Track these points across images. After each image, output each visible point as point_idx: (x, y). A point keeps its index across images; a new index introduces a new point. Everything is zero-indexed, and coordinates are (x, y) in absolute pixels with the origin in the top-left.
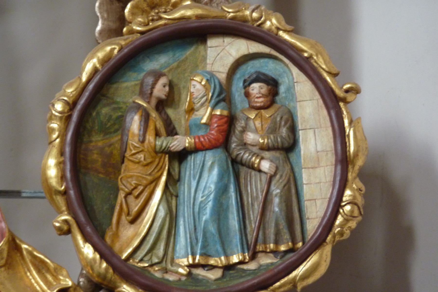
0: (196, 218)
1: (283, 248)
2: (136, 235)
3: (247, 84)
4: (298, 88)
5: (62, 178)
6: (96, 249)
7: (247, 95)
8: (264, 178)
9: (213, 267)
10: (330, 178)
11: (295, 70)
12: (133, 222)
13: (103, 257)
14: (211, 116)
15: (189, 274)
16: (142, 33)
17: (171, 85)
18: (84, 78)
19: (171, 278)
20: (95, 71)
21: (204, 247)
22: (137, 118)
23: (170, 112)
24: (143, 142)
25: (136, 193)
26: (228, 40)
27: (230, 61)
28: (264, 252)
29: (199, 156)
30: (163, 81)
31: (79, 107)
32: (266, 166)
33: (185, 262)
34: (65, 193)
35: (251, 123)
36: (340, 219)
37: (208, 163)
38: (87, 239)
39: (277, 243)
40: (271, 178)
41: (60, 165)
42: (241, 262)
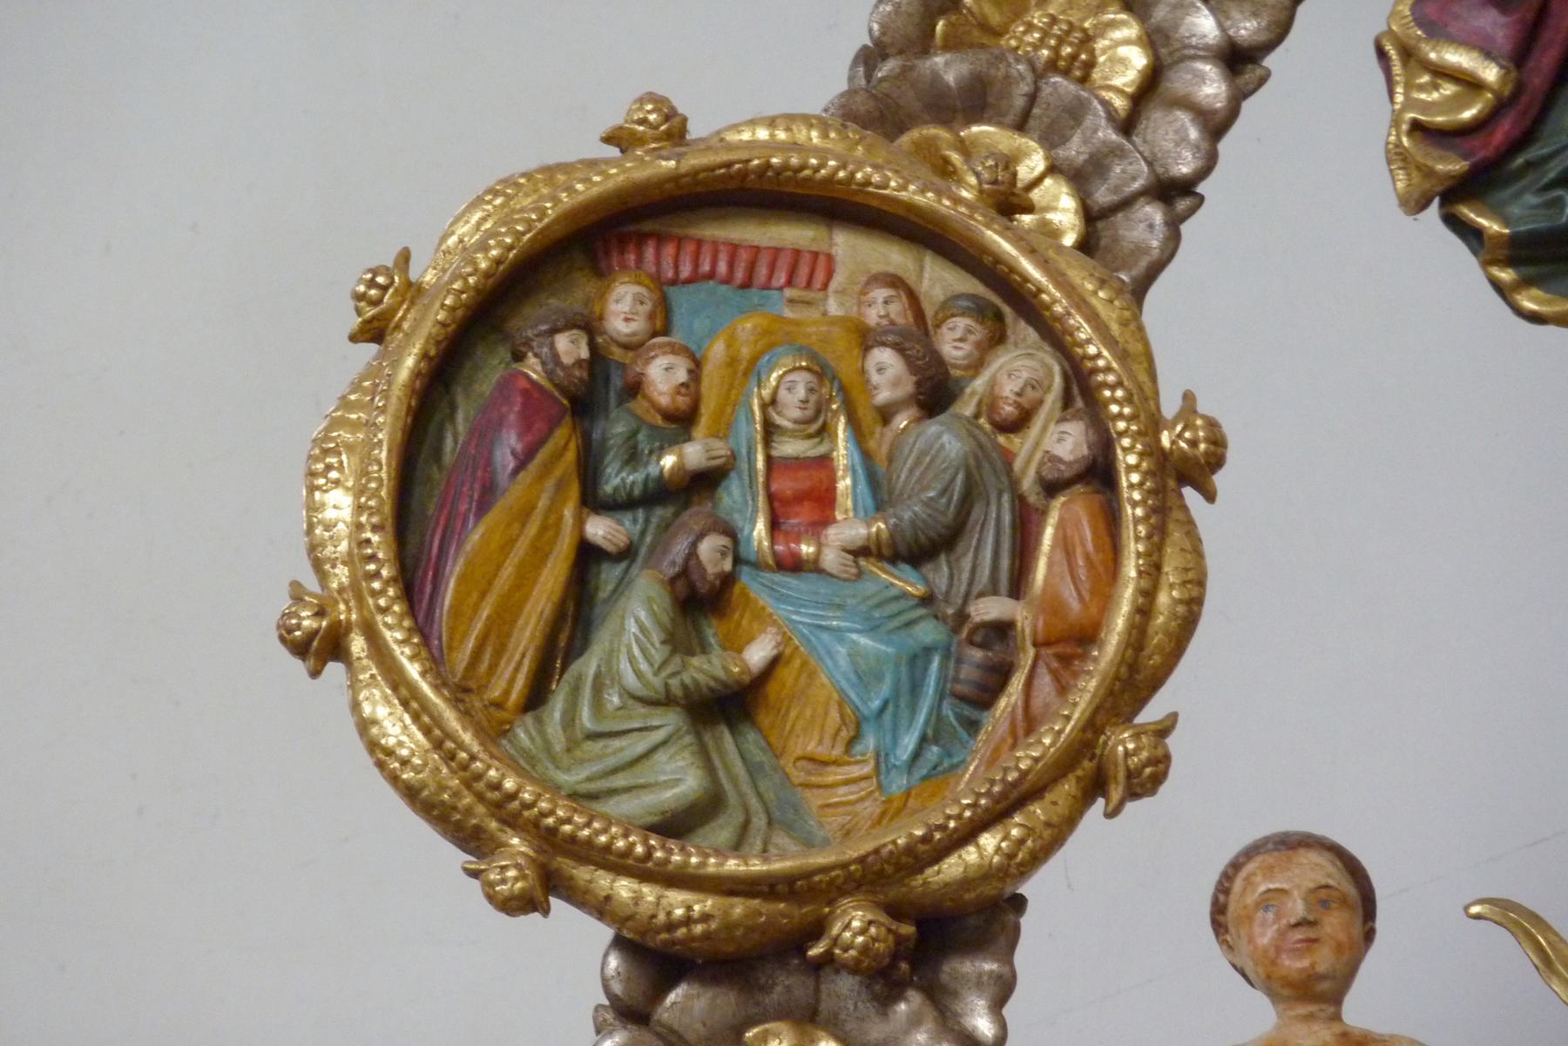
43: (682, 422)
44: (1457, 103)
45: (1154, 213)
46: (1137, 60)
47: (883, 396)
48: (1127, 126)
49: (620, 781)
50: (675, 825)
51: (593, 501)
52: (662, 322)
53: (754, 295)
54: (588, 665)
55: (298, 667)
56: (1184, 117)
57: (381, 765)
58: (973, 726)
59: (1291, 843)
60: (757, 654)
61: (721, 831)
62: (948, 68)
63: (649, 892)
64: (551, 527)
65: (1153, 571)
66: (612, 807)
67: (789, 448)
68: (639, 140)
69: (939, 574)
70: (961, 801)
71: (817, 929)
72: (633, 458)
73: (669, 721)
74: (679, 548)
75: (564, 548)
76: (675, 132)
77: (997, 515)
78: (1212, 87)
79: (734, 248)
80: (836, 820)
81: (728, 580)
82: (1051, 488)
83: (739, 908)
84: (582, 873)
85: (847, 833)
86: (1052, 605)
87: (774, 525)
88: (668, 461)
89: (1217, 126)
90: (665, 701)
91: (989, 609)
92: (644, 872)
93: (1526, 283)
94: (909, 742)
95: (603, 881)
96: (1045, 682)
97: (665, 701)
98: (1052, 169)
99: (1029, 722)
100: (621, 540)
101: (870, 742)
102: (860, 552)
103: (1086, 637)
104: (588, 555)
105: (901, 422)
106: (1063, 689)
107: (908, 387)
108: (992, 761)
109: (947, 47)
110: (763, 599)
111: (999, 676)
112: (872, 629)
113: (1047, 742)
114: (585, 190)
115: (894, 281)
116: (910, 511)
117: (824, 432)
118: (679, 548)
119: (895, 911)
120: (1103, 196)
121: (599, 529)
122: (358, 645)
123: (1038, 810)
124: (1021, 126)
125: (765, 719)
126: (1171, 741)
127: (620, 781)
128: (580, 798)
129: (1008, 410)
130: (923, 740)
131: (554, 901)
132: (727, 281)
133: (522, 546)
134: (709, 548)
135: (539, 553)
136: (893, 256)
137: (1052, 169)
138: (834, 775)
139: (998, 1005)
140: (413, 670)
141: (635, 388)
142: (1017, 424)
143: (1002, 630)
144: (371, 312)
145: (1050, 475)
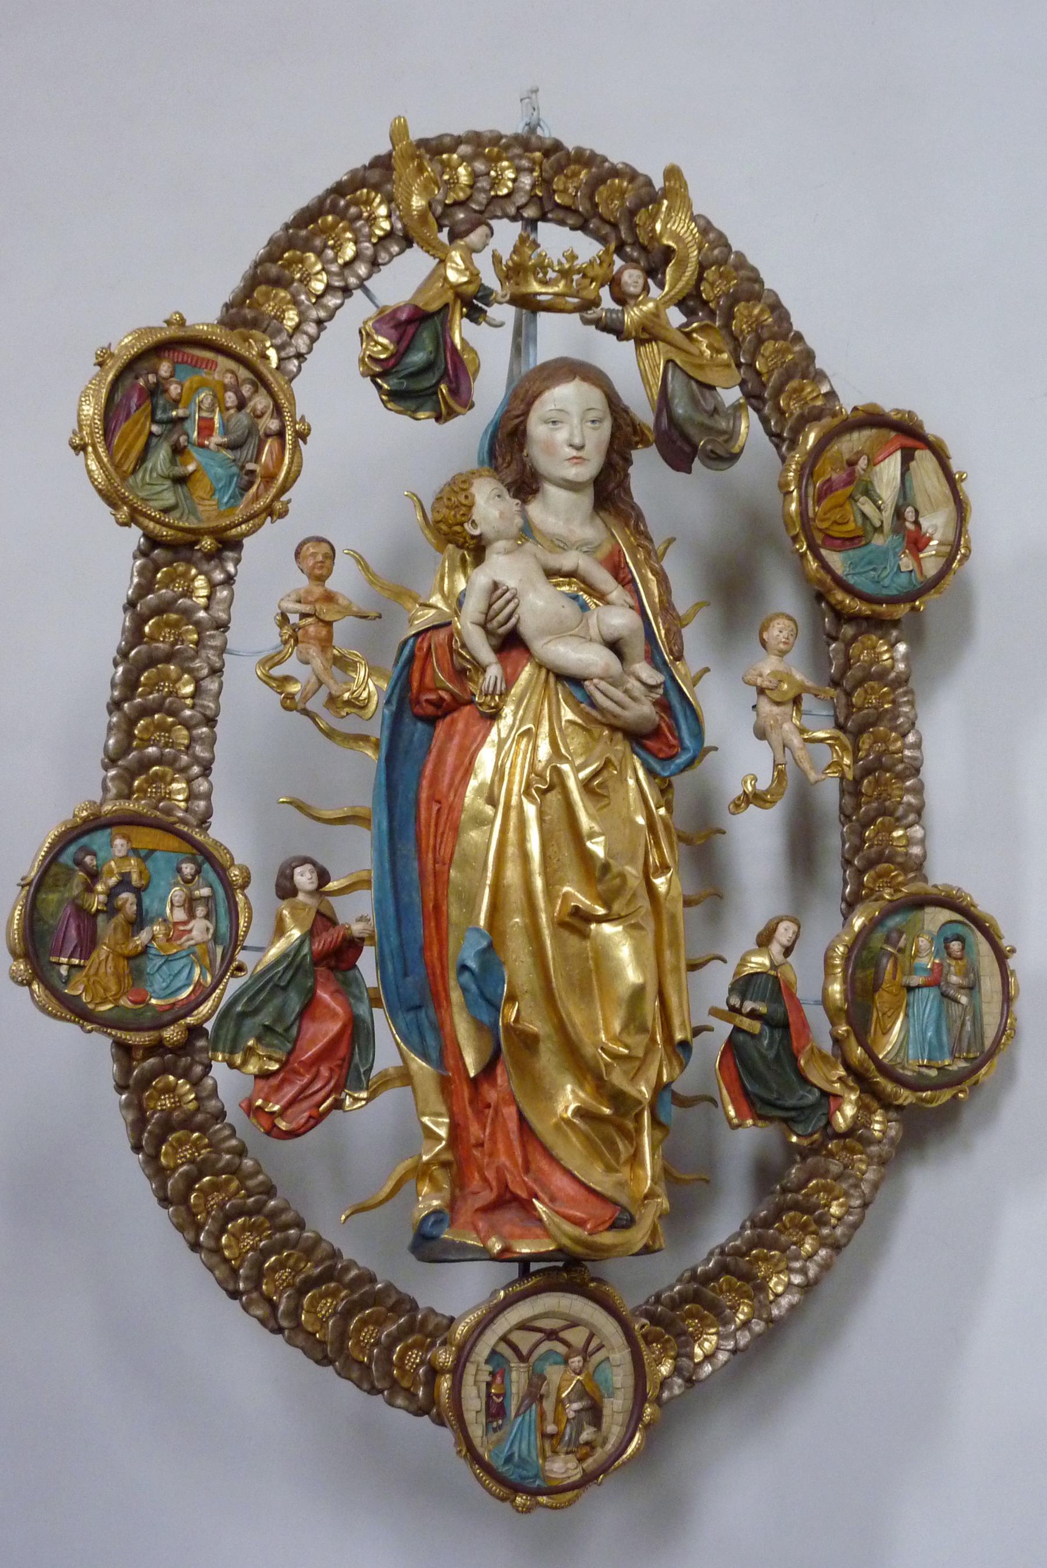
1: (972, 1056)
5: (846, 999)
11: (979, 934)
14: (934, 964)
16: (890, 901)
19: (909, 1073)
21: (929, 1053)
24: (894, 978)
25: (889, 1014)
26: (938, 909)
31: (855, 952)
32: (964, 1000)
35: (952, 968)
36: (1004, 1037)
37: (932, 996)
39: (968, 1052)
44: (380, 352)
45: (296, 362)
47: (229, 404)
48: (291, 337)
49: (154, 497)
50: (166, 511)
51: (154, 421)
53: (197, 369)
54: (149, 465)
55: (72, 451)
56: (305, 336)
57: (93, 483)
58: (242, 495)
59: (320, 540)
60: (191, 468)
61: (177, 514)
62: (249, 313)
63: (158, 527)
64: (144, 424)
65: (291, 462)
66: (151, 503)
67: (205, 414)
68: (173, 324)
69: (238, 453)
70: (238, 515)
71: (197, 542)
72: (164, 411)
73: (168, 483)
74: (175, 437)
75: (146, 432)
76: (182, 323)
77: (253, 442)
79: (193, 356)
80: (206, 514)
81: (185, 447)
82: (268, 436)
83: (180, 534)
84: (141, 519)
85: (208, 518)
88: (174, 413)
89: (313, 339)
90: (167, 478)
91: (250, 466)
92: (158, 521)
93: (389, 401)
94: (225, 499)
95: (146, 522)
96: (262, 487)
97: (167, 478)
98: (272, 346)
99: (257, 497)
100: (160, 432)
101: (217, 497)
102: (219, 445)
104: (151, 434)
105: (232, 411)
107: (236, 403)
108: (246, 506)
109: (249, 307)
110: (195, 455)
111: (250, 484)
112: (221, 467)
113: (262, 503)
114: (160, 336)
115: (233, 372)
116: (233, 437)
117: (213, 411)
118: (175, 437)
120: (283, 354)
121: (155, 429)
122: (90, 449)
123: (256, 520)
124: (264, 332)
125: (189, 484)
126: (289, 505)
127: (154, 497)
128: (144, 500)
129: (259, 413)
130: (230, 498)
131: (133, 525)
132: (191, 364)
133: (136, 431)
134: (182, 439)
135: (140, 433)
136: (232, 364)
137: (272, 346)
138: (207, 502)
139: (236, 564)
140: (105, 460)
141: (166, 391)
142: (260, 417)
143: (252, 472)
144: (101, 359)
145: (268, 431)
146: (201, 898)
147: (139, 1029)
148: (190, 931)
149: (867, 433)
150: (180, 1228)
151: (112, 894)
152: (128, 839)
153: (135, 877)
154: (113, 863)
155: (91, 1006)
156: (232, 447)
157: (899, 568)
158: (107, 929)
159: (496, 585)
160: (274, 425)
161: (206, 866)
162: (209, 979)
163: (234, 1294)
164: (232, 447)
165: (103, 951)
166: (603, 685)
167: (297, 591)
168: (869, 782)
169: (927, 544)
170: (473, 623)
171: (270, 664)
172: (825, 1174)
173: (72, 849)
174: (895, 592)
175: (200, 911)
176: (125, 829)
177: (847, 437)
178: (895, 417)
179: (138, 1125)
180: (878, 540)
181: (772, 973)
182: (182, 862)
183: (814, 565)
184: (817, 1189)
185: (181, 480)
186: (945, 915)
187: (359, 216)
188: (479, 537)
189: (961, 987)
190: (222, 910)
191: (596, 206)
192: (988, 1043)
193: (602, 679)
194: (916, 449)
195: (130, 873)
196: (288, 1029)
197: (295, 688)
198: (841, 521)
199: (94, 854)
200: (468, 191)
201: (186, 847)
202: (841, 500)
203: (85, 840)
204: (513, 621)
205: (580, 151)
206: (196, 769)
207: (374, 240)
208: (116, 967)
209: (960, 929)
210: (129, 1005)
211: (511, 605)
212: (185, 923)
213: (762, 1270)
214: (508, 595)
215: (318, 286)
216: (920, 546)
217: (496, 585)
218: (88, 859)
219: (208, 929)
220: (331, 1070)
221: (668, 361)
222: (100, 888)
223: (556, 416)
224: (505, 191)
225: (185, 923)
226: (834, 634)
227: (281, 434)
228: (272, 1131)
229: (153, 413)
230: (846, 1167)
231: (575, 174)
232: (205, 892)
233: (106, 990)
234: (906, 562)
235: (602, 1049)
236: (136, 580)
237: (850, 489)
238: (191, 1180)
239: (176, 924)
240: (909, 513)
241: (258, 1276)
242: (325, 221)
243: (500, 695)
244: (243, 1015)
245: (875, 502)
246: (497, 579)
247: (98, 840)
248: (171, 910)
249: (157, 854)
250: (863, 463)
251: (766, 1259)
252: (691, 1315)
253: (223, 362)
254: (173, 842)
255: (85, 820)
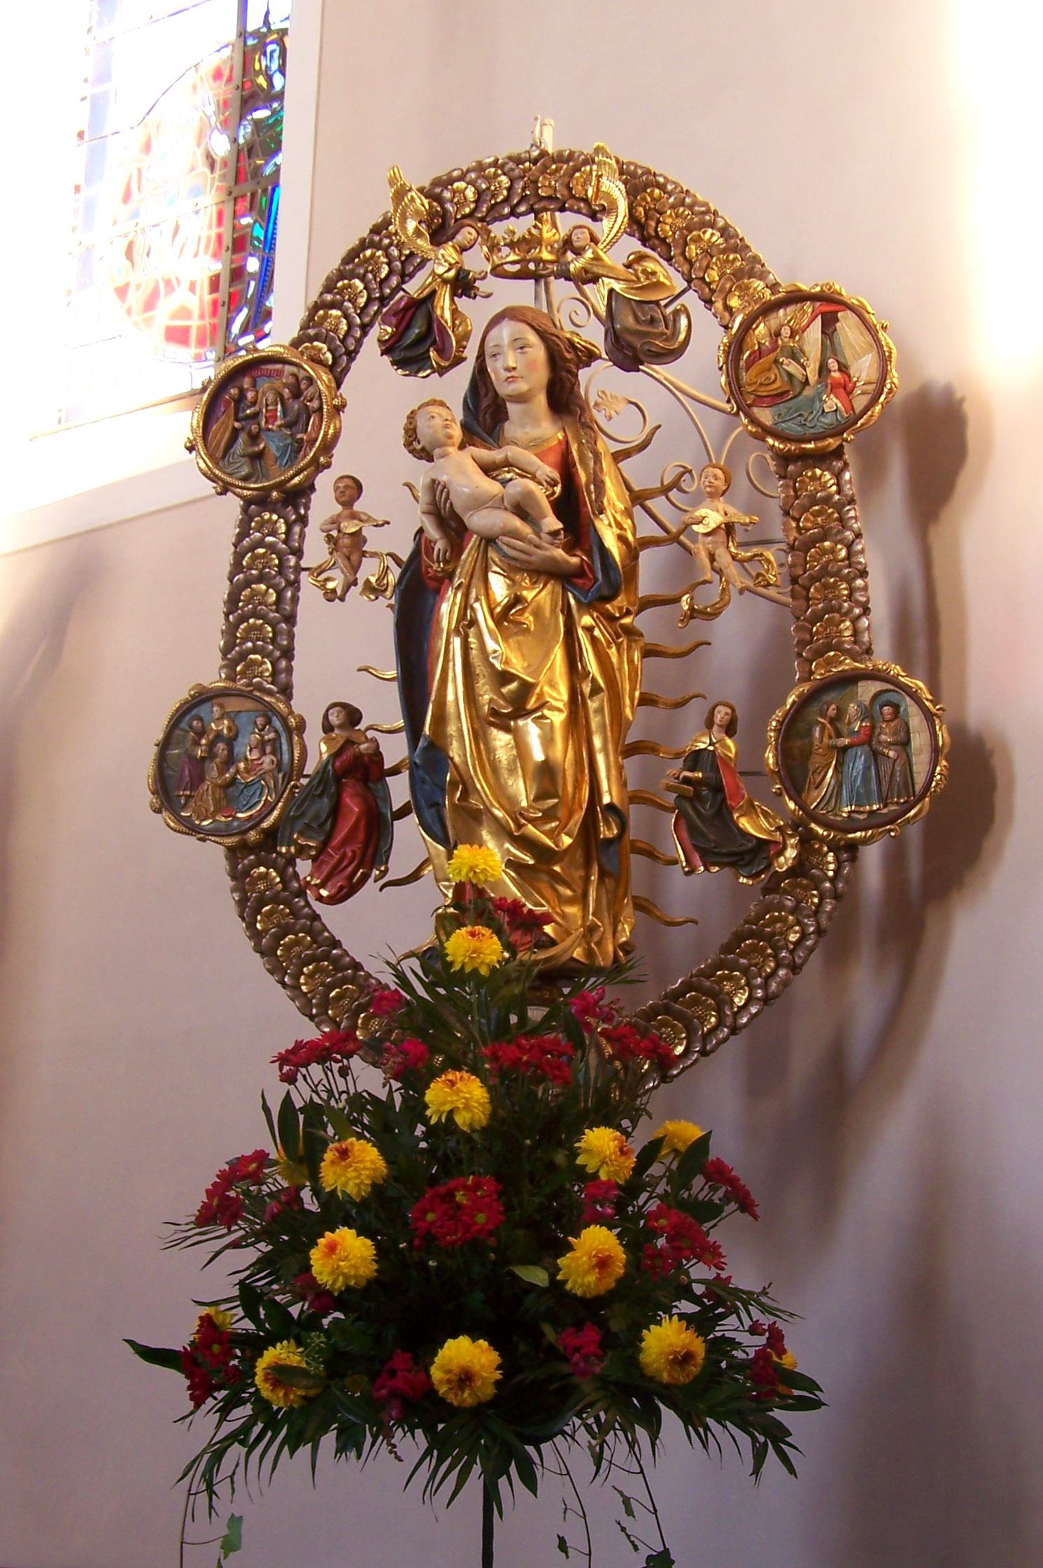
0: (852, 784)
2: (819, 795)
3: (881, 707)
4: (910, 709)
6: (796, 804)
7: (881, 713)
8: (891, 761)
9: (862, 813)
10: (928, 760)
11: (908, 699)
12: (817, 788)
13: (800, 808)
14: (861, 727)
15: (849, 817)
17: (838, 708)
18: (788, 707)
20: (794, 702)
22: (818, 729)
23: (839, 726)
24: (821, 742)
26: (869, 682)
27: (871, 694)
28: (892, 803)
29: (854, 749)
30: (833, 706)
32: (892, 754)
33: (847, 809)
34: (778, 772)
36: (934, 784)
38: (791, 799)
39: (899, 798)
40: (895, 761)
41: (776, 756)
42: (878, 809)
43: (254, 404)
46: (345, 328)
50: (245, 479)
51: (237, 420)
52: (254, 385)
54: (232, 450)
58: (296, 458)
60: (262, 446)
67: (270, 408)
75: (230, 428)
78: (358, 333)
82: (314, 412)
83: (255, 493)
86: (309, 436)
87: (267, 422)
88: (248, 411)
90: (243, 456)
91: (299, 436)
97: (243, 456)
102: (280, 426)
103: (316, 440)
104: (234, 428)
106: (311, 450)
116: (288, 418)
119: (283, 492)
120: (337, 355)
121: (237, 425)
124: (324, 343)
143: (302, 439)
146: (269, 740)
147: (229, 836)
148: (262, 764)
149: (790, 309)
150: (271, 972)
151: (211, 745)
152: (221, 706)
153: (225, 731)
154: (213, 725)
155: (197, 822)
156: (289, 426)
157: (823, 411)
158: (212, 771)
159: (433, 481)
160: (315, 404)
161: (274, 718)
162: (274, 796)
163: (312, 1017)
164: (289, 426)
165: (207, 784)
166: (505, 539)
167: (332, 517)
168: (815, 589)
169: (854, 386)
170: (423, 513)
171: (319, 571)
172: (781, 907)
173: (187, 718)
174: (821, 430)
175: (268, 749)
176: (219, 700)
177: (774, 315)
178: (813, 291)
179: (242, 903)
180: (808, 392)
181: (711, 748)
182: (257, 717)
183: (746, 421)
184: (775, 920)
185: (259, 456)
186: (875, 687)
187: (391, 244)
188: (423, 449)
189: (890, 744)
190: (285, 747)
191: (570, 189)
192: (918, 787)
193: (504, 535)
194: (837, 312)
195: (222, 730)
196: (321, 825)
197: (330, 585)
198: (767, 382)
199: (201, 720)
200: (472, 206)
201: (260, 707)
202: (766, 366)
203: (195, 712)
204: (448, 505)
205: (560, 154)
206: (278, 653)
207: (403, 258)
208: (213, 793)
209: (893, 697)
210: (223, 819)
211: (444, 494)
212: (259, 759)
213: (728, 987)
214: (440, 487)
215: (362, 301)
216: (849, 389)
217: (433, 481)
218: (195, 723)
219: (273, 761)
220: (354, 852)
221: (611, 291)
222: (204, 741)
223: (496, 350)
224: (501, 198)
225: (259, 759)
226: (783, 474)
227: (321, 409)
228: (320, 898)
229: (236, 413)
230: (798, 902)
231: (557, 170)
232: (272, 735)
233: (207, 811)
234: (832, 402)
235: (521, 814)
236: (238, 530)
237: (772, 356)
238: (278, 938)
239: (253, 760)
240: (832, 364)
241: (325, 1003)
242: (364, 256)
243: (446, 562)
244: (295, 819)
245: (799, 362)
246: (434, 477)
247: (203, 711)
248: (251, 751)
249: (243, 714)
250: (786, 331)
251: (730, 978)
252: (663, 1024)
253: (288, 369)
254: (249, 704)
255: (193, 697)
